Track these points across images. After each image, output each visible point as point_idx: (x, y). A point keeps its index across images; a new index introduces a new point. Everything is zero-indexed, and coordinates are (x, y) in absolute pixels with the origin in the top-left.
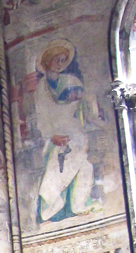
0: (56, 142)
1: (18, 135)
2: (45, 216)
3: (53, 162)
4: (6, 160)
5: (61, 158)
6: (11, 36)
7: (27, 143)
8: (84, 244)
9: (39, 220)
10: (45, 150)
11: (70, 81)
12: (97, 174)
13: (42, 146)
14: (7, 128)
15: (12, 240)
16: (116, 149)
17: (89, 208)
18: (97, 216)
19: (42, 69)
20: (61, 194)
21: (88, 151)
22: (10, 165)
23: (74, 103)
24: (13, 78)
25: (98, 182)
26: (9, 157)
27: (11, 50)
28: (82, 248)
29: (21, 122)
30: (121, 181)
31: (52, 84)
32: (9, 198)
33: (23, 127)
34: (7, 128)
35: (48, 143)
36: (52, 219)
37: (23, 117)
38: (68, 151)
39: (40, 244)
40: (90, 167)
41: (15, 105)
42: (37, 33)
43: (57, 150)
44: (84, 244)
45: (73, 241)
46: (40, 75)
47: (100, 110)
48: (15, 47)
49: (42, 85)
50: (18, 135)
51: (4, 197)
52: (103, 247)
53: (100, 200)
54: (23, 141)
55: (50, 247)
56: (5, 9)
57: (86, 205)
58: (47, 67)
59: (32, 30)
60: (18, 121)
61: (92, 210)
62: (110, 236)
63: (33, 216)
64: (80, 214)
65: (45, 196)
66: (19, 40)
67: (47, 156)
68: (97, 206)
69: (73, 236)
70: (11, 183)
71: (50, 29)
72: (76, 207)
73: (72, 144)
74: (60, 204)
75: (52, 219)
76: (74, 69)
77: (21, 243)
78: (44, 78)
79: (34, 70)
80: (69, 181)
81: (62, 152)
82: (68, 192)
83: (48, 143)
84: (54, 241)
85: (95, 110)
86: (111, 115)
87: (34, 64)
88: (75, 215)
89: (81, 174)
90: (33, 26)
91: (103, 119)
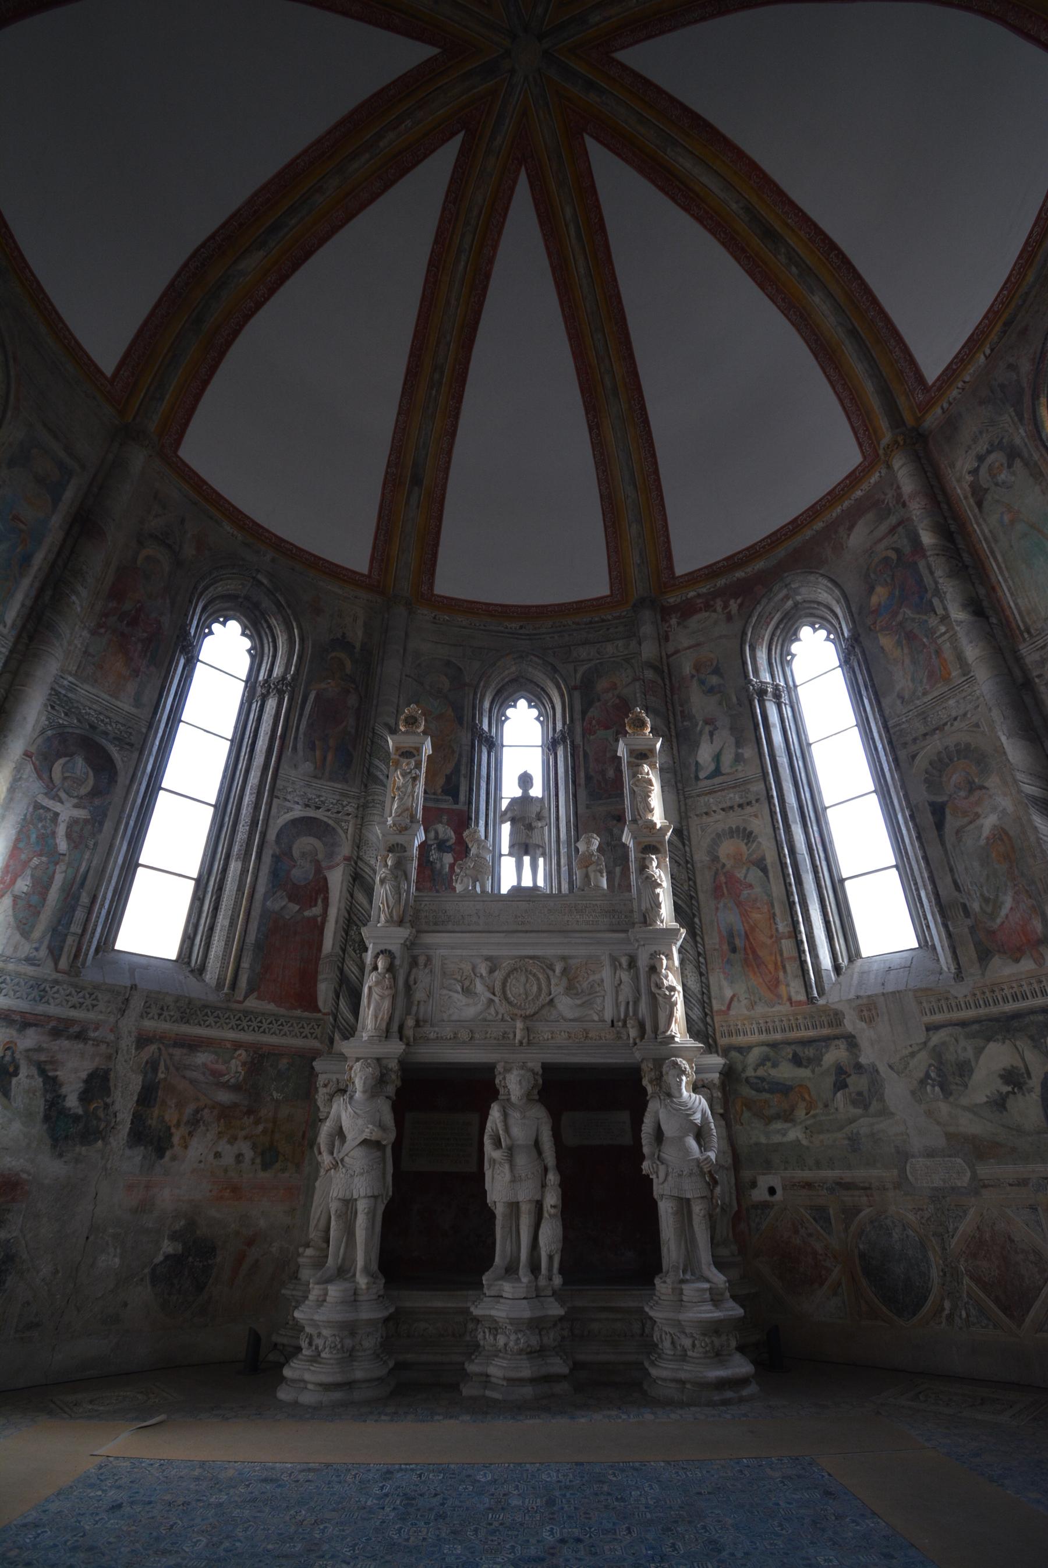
0: (707, 722)
1: (679, 718)
2: (702, 775)
3: (705, 737)
4: (671, 736)
5: (711, 734)
6: (671, 650)
7: (685, 723)
8: (732, 795)
9: (697, 778)
10: (699, 728)
11: (714, 680)
12: (738, 744)
13: (697, 725)
14: (671, 715)
15: (678, 793)
16: (752, 727)
17: (734, 769)
18: (741, 775)
19: (694, 672)
20: (713, 760)
21: (731, 729)
22: (674, 740)
23: (719, 695)
24: (673, 678)
25: (740, 751)
26: (673, 734)
27: (671, 659)
28: (731, 798)
29: (680, 708)
30: (757, 750)
31: (702, 682)
32: (674, 763)
33: (682, 712)
34: (670, 712)
35: (701, 723)
36: (707, 778)
37: (681, 705)
38: (716, 729)
39: (698, 796)
40: (732, 740)
41: (676, 697)
42: (689, 648)
43: (708, 728)
44: (732, 795)
45: (723, 793)
46: (693, 676)
47: (738, 699)
48: (674, 657)
49: (695, 685)
50: (679, 718)
51: (671, 762)
52: (747, 798)
53: (742, 763)
54: (682, 722)
55: (706, 799)
56: (666, 631)
57: (731, 767)
58: (698, 671)
59: (686, 645)
60: (679, 709)
61: (737, 770)
62: (751, 789)
63: (692, 776)
64: (728, 774)
65: (700, 760)
66: (677, 652)
67: (701, 732)
68: (740, 768)
69: (723, 790)
70: (675, 752)
71: (698, 645)
72: (726, 767)
73: (718, 724)
74: (712, 767)
75: (707, 778)
76: (717, 671)
77: (684, 795)
78: (695, 678)
79: (688, 672)
80: (718, 750)
81: (711, 729)
82: (717, 758)
83: (701, 723)
84: (710, 793)
85: (734, 699)
86: (746, 702)
87: (688, 669)
88: (724, 775)
89: (727, 745)
90: (686, 643)
91: (741, 706)
